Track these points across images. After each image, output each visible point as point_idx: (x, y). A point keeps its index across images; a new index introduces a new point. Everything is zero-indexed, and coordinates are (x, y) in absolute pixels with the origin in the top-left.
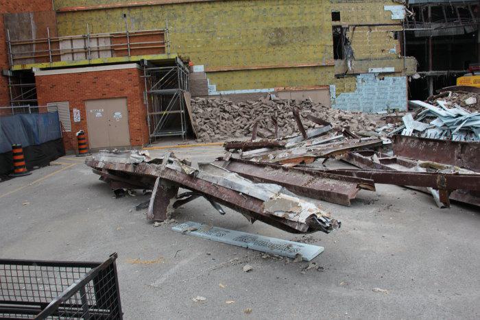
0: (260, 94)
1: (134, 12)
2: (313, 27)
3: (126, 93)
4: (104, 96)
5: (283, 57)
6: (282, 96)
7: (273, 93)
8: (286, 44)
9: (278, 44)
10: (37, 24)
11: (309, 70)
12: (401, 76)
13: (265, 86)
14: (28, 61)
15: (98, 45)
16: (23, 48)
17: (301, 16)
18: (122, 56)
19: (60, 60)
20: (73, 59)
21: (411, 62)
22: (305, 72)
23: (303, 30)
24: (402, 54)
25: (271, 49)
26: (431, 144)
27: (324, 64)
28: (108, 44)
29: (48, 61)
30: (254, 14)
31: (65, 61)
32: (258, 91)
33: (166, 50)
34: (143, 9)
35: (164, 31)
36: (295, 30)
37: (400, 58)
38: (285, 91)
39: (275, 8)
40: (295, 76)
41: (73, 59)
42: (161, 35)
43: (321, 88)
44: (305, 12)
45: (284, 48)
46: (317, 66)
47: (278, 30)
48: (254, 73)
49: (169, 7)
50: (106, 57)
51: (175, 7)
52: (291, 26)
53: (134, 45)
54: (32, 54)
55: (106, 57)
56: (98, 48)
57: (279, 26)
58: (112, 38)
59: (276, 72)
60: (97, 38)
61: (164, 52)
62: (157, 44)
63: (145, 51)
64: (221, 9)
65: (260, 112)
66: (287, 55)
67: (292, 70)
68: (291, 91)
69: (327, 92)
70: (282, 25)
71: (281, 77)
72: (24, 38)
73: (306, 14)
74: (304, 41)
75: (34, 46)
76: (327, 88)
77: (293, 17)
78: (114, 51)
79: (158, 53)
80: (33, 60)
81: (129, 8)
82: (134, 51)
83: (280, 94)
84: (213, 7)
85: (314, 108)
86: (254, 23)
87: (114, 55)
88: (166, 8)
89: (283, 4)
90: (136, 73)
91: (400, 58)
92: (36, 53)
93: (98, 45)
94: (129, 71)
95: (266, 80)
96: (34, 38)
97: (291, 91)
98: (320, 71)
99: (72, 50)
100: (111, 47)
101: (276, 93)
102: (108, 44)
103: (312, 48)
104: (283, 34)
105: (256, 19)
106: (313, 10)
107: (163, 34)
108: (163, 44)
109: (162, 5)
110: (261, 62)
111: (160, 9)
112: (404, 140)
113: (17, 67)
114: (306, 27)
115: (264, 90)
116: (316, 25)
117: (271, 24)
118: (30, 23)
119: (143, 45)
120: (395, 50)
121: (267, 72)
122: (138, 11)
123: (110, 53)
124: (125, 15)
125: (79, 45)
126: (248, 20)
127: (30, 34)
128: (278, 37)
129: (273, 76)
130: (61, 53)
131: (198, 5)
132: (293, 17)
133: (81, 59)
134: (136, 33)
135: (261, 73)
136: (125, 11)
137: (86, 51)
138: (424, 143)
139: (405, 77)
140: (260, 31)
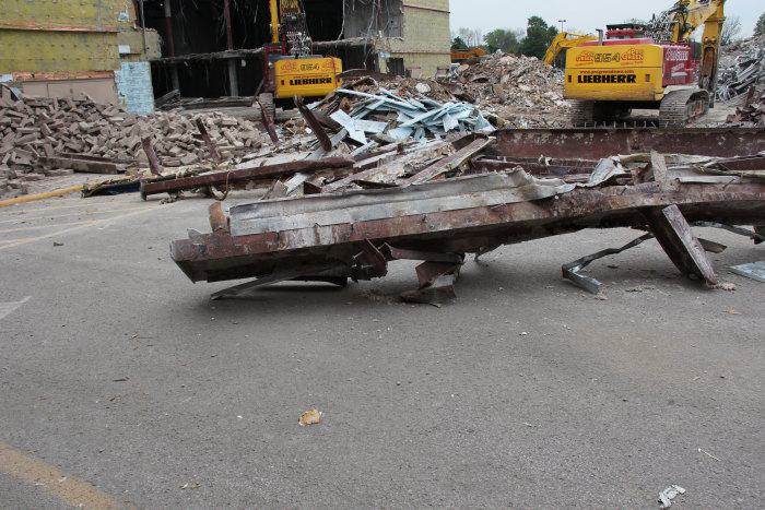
6: (34, 92)
11: (76, 40)
12: (140, 61)
21: (152, 37)
22: (68, 41)
24: (139, 23)
26: (530, 136)
27: (100, 29)
37: (136, 30)
38: (33, 80)
40: (53, 50)
43: (98, 76)
46: (105, 33)
65: (8, 125)
68: (47, 81)
69: (110, 84)
76: (109, 75)
83: (26, 87)
85: (105, 112)
91: (136, 30)
97: (47, 81)
98: (94, 42)
101: (19, 83)
112: (518, 137)
120: (126, 15)
138: (564, 136)
139: (147, 64)
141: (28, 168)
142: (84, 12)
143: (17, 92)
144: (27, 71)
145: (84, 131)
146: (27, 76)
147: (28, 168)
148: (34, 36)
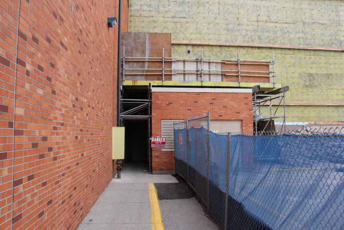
0: (297, 125)
1: (196, 49)
2: (336, 74)
3: (241, 116)
4: (221, 118)
5: (313, 97)
7: (307, 125)
8: (316, 86)
9: (311, 86)
10: (152, 44)
11: (333, 109)
13: (300, 120)
14: (138, 77)
15: (209, 68)
16: (135, 64)
17: (326, 65)
18: (231, 81)
19: (170, 79)
20: (184, 80)
22: (330, 109)
23: (328, 76)
25: (305, 90)
28: (218, 69)
29: (162, 80)
30: (293, 61)
31: (176, 80)
32: (295, 123)
33: (271, 79)
34: (205, 48)
35: (269, 63)
36: (322, 75)
38: (315, 124)
39: (308, 57)
40: (325, 113)
41: (184, 80)
42: (267, 65)
44: (330, 62)
45: (315, 90)
47: (311, 75)
48: (292, 108)
49: (227, 49)
50: (217, 81)
51: (231, 49)
52: (320, 73)
53: (243, 73)
54: (143, 71)
55: (217, 81)
56: (184, 71)
57: (311, 72)
58: (223, 64)
59: (309, 109)
60: (209, 63)
61: (269, 82)
62: (264, 74)
63: (253, 79)
64: (267, 54)
66: (317, 95)
67: (320, 108)
70: (314, 71)
71: (312, 113)
72: (137, 56)
73: (330, 64)
74: (330, 85)
75: (147, 64)
77: (322, 65)
78: (224, 75)
79: (264, 82)
80: (144, 77)
81: (193, 45)
82: (249, 78)
84: (261, 52)
86: (292, 68)
87: (224, 79)
88: (223, 49)
89: (314, 55)
90: (251, 98)
92: (147, 71)
93: (209, 68)
94: (246, 96)
95: (301, 115)
96: (147, 57)
99: (210, 72)
100: (222, 72)
101: (310, 125)
102: (218, 69)
103: (335, 91)
104: (314, 78)
105: (294, 65)
106: (335, 61)
107: (268, 65)
108: (269, 74)
109: (221, 46)
110: (297, 100)
111: (218, 49)
113: (128, 83)
114: (331, 74)
115: (300, 124)
116: (338, 73)
117: (305, 70)
118: (145, 42)
119: (251, 73)
121: (302, 108)
122: (200, 49)
123: (220, 77)
124: (189, 52)
125: (191, 67)
126: (288, 65)
127: (143, 53)
128: (310, 80)
129: (307, 111)
130: (173, 73)
131: (250, 50)
132: (322, 65)
133: (192, 80)
134: (244, 62)
135: (297, 108)
136: (190, 48)
137: (199, 74)
140: (297, 75)
141: (311, 158)
142: (338, 98)
143: (308, 129)
144: (313, 121)
145: (333, 146)
146: (313, 123)
147: (311, 158)
148: (317, 108)
